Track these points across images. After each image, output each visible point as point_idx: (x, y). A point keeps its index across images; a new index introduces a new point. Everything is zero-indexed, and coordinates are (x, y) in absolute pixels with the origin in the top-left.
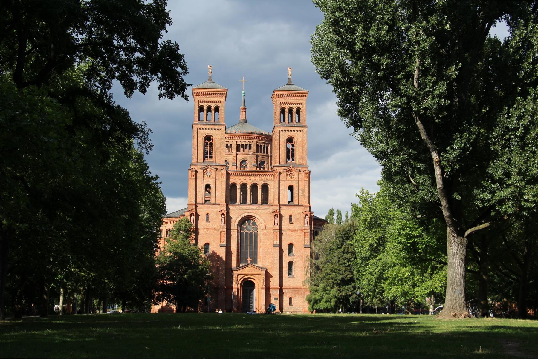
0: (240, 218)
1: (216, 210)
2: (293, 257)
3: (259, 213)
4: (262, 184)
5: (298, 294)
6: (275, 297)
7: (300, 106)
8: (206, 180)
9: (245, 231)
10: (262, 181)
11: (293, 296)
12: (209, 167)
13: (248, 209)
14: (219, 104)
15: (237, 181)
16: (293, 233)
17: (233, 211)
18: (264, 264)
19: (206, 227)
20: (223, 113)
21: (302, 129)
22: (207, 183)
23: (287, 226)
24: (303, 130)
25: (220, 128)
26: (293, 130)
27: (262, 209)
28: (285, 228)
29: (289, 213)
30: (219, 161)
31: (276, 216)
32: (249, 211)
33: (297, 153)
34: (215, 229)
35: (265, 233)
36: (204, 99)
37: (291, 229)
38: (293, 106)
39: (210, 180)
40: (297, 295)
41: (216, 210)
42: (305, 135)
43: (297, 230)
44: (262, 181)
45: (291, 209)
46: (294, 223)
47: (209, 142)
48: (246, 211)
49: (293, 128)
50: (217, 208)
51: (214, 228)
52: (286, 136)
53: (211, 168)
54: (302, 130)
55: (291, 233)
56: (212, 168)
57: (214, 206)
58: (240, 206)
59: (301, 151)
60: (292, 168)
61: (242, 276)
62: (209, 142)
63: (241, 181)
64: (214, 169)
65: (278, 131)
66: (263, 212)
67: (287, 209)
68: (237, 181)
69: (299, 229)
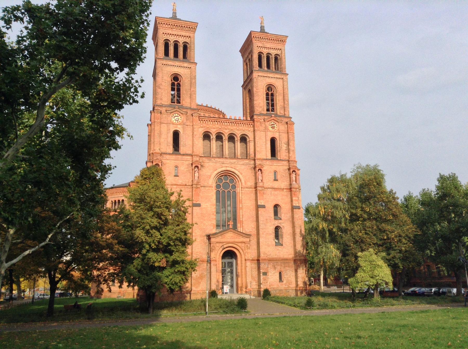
0: (216, 172)
1: (187, 163)
2: (280, 221)
3: (238, 169)
4: (240, 135)
5: (289, 267)
6: (263, 271)
9: (222, 189)
10: (240, 132)
11: (283, 269)
12: (178, 110)
13: (225, 163)
15: (211, 129)
16: (278, 192)
17: (207, 165)
18: (247, 230)
19: (174, 183)
21: (282, 76)
22: (175, 129)
23: (271, 184)
24: (284, 78)
25: (189, 67)
26: (272, 77)
27: (241, 163)
28: (269, 187)
29: (274, 168)
30: (189, 105)
31: (260, 171)
32: (227, 165)
34: (186, 185)
35: (246, 192)
36: (170, 32)
37: (276, 187)
39: (179, 126)
40: (288, 268)
41: (187, 163)
43: (283, 189)
44: (240, 132)
45: (275, 164)
46: (279, 181)
47: (176, 83)
48: (223, 165)
50: (188, 160)
51: (184, 183)
52: (265, 83)
53: (180, 111)
54: (282, 78)
55: (276, 193)
56: (181, 112)
57: (184, 157)
58: (216, 160)
60: (274, 118)
61: (222, 244)
63: (216, 130)
66: (243, 167)
67: (271, 164)
68: (211, 129)
69: (285, 188)
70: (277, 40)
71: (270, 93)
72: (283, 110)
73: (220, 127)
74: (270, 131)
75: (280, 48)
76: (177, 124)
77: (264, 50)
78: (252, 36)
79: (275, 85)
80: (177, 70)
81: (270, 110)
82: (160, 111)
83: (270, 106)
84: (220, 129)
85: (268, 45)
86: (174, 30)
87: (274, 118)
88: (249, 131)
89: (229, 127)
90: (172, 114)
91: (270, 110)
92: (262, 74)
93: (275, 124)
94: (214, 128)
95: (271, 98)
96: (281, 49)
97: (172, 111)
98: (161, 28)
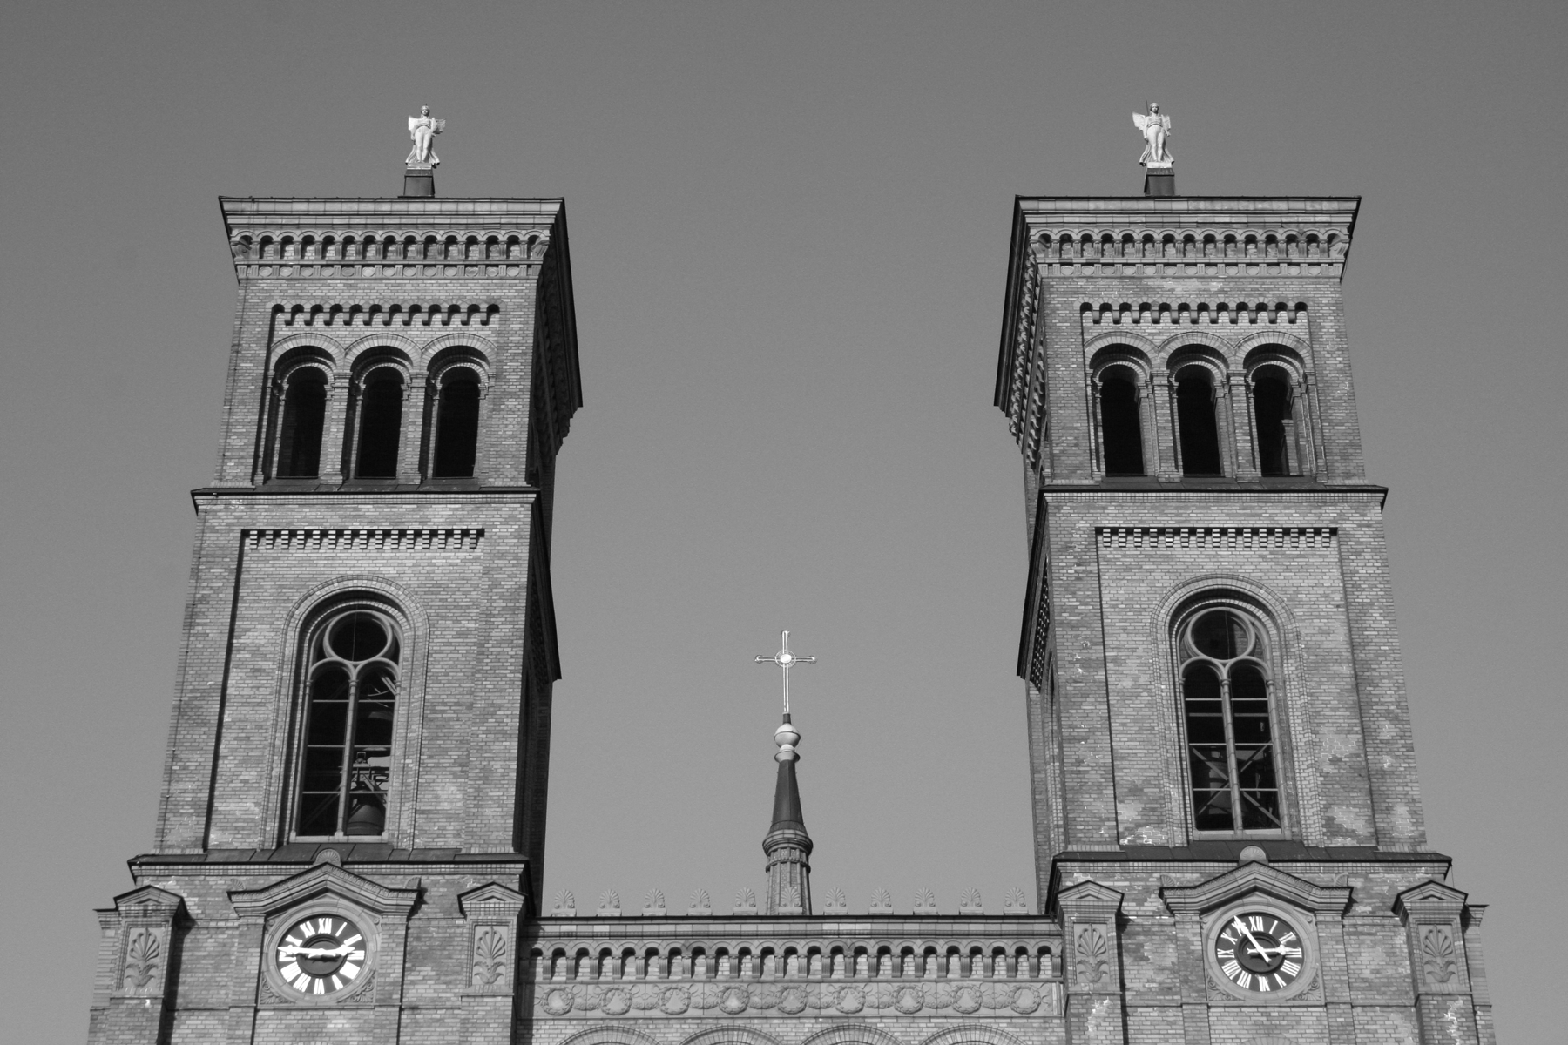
7: (1286, 331)
8: (292, 1019)
14: (476, 335)
20: (512, 403)
21: (1328, 515)
24: (1348, 526)
26: (1231, 524)
33: (1300, 737)
36: (335, 290)
38: (1220, 333)
42: (1365, 568)
49: (1236, 508)
53: (353, 885)
56: (367, 893)
59: (1344, 718)
62: (354, 668)
64: (384, 899)
65: (1080, 538)
70: (1261, 235)
71: (1223, 668)
72: (1361, 798)
73: (734, 1003)
74: (1234, 1004)
75: (1291, 294)
76: (330, 1000)
77: (1146, 327)
78: (1035, 234)
79: (1262, 595)
80: (365, 567)
81: (1237, 810)
82: (168, 903)
83: (1234, 777)
84: (734, 1014)
85: (1180, 288)
86: (368, 272)
87: (1263, 876)
88: (1026, 1014)
89: (826, 993)
90: (281, 923)
91: (1237, 810)
92: (1129, 510)
93: (1286, 927)
94: (671, 1016)
95: (1236, 707)
96: (1301, 307)
97: (282, 894)
98: (266, 272)
